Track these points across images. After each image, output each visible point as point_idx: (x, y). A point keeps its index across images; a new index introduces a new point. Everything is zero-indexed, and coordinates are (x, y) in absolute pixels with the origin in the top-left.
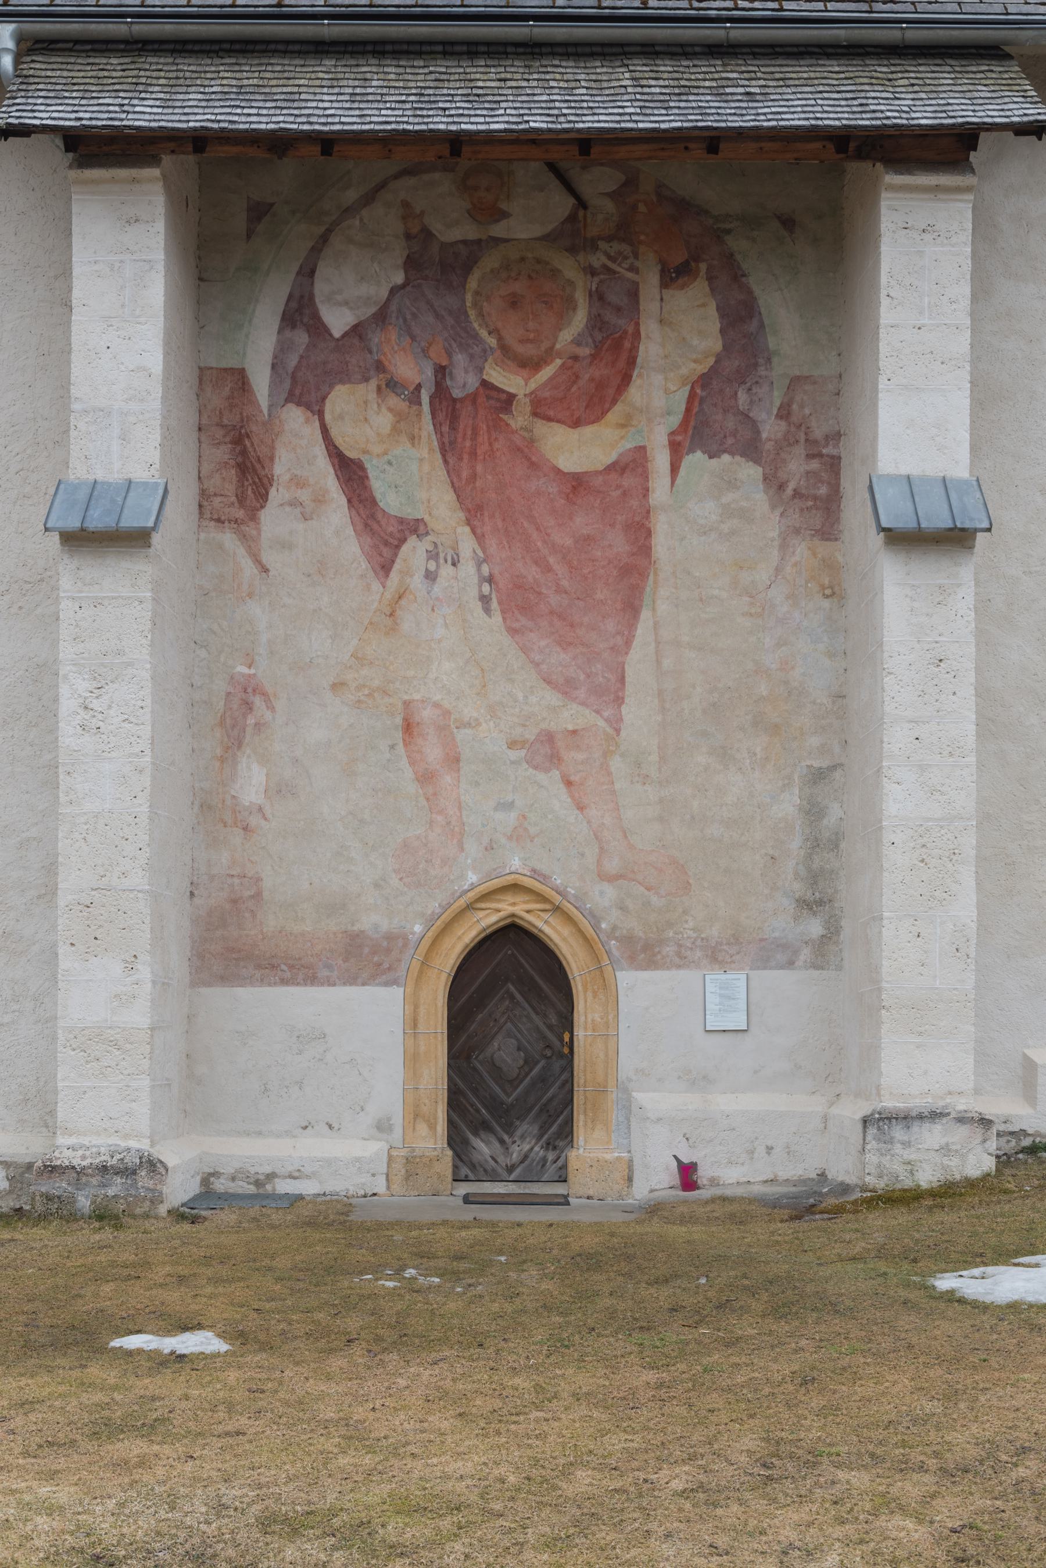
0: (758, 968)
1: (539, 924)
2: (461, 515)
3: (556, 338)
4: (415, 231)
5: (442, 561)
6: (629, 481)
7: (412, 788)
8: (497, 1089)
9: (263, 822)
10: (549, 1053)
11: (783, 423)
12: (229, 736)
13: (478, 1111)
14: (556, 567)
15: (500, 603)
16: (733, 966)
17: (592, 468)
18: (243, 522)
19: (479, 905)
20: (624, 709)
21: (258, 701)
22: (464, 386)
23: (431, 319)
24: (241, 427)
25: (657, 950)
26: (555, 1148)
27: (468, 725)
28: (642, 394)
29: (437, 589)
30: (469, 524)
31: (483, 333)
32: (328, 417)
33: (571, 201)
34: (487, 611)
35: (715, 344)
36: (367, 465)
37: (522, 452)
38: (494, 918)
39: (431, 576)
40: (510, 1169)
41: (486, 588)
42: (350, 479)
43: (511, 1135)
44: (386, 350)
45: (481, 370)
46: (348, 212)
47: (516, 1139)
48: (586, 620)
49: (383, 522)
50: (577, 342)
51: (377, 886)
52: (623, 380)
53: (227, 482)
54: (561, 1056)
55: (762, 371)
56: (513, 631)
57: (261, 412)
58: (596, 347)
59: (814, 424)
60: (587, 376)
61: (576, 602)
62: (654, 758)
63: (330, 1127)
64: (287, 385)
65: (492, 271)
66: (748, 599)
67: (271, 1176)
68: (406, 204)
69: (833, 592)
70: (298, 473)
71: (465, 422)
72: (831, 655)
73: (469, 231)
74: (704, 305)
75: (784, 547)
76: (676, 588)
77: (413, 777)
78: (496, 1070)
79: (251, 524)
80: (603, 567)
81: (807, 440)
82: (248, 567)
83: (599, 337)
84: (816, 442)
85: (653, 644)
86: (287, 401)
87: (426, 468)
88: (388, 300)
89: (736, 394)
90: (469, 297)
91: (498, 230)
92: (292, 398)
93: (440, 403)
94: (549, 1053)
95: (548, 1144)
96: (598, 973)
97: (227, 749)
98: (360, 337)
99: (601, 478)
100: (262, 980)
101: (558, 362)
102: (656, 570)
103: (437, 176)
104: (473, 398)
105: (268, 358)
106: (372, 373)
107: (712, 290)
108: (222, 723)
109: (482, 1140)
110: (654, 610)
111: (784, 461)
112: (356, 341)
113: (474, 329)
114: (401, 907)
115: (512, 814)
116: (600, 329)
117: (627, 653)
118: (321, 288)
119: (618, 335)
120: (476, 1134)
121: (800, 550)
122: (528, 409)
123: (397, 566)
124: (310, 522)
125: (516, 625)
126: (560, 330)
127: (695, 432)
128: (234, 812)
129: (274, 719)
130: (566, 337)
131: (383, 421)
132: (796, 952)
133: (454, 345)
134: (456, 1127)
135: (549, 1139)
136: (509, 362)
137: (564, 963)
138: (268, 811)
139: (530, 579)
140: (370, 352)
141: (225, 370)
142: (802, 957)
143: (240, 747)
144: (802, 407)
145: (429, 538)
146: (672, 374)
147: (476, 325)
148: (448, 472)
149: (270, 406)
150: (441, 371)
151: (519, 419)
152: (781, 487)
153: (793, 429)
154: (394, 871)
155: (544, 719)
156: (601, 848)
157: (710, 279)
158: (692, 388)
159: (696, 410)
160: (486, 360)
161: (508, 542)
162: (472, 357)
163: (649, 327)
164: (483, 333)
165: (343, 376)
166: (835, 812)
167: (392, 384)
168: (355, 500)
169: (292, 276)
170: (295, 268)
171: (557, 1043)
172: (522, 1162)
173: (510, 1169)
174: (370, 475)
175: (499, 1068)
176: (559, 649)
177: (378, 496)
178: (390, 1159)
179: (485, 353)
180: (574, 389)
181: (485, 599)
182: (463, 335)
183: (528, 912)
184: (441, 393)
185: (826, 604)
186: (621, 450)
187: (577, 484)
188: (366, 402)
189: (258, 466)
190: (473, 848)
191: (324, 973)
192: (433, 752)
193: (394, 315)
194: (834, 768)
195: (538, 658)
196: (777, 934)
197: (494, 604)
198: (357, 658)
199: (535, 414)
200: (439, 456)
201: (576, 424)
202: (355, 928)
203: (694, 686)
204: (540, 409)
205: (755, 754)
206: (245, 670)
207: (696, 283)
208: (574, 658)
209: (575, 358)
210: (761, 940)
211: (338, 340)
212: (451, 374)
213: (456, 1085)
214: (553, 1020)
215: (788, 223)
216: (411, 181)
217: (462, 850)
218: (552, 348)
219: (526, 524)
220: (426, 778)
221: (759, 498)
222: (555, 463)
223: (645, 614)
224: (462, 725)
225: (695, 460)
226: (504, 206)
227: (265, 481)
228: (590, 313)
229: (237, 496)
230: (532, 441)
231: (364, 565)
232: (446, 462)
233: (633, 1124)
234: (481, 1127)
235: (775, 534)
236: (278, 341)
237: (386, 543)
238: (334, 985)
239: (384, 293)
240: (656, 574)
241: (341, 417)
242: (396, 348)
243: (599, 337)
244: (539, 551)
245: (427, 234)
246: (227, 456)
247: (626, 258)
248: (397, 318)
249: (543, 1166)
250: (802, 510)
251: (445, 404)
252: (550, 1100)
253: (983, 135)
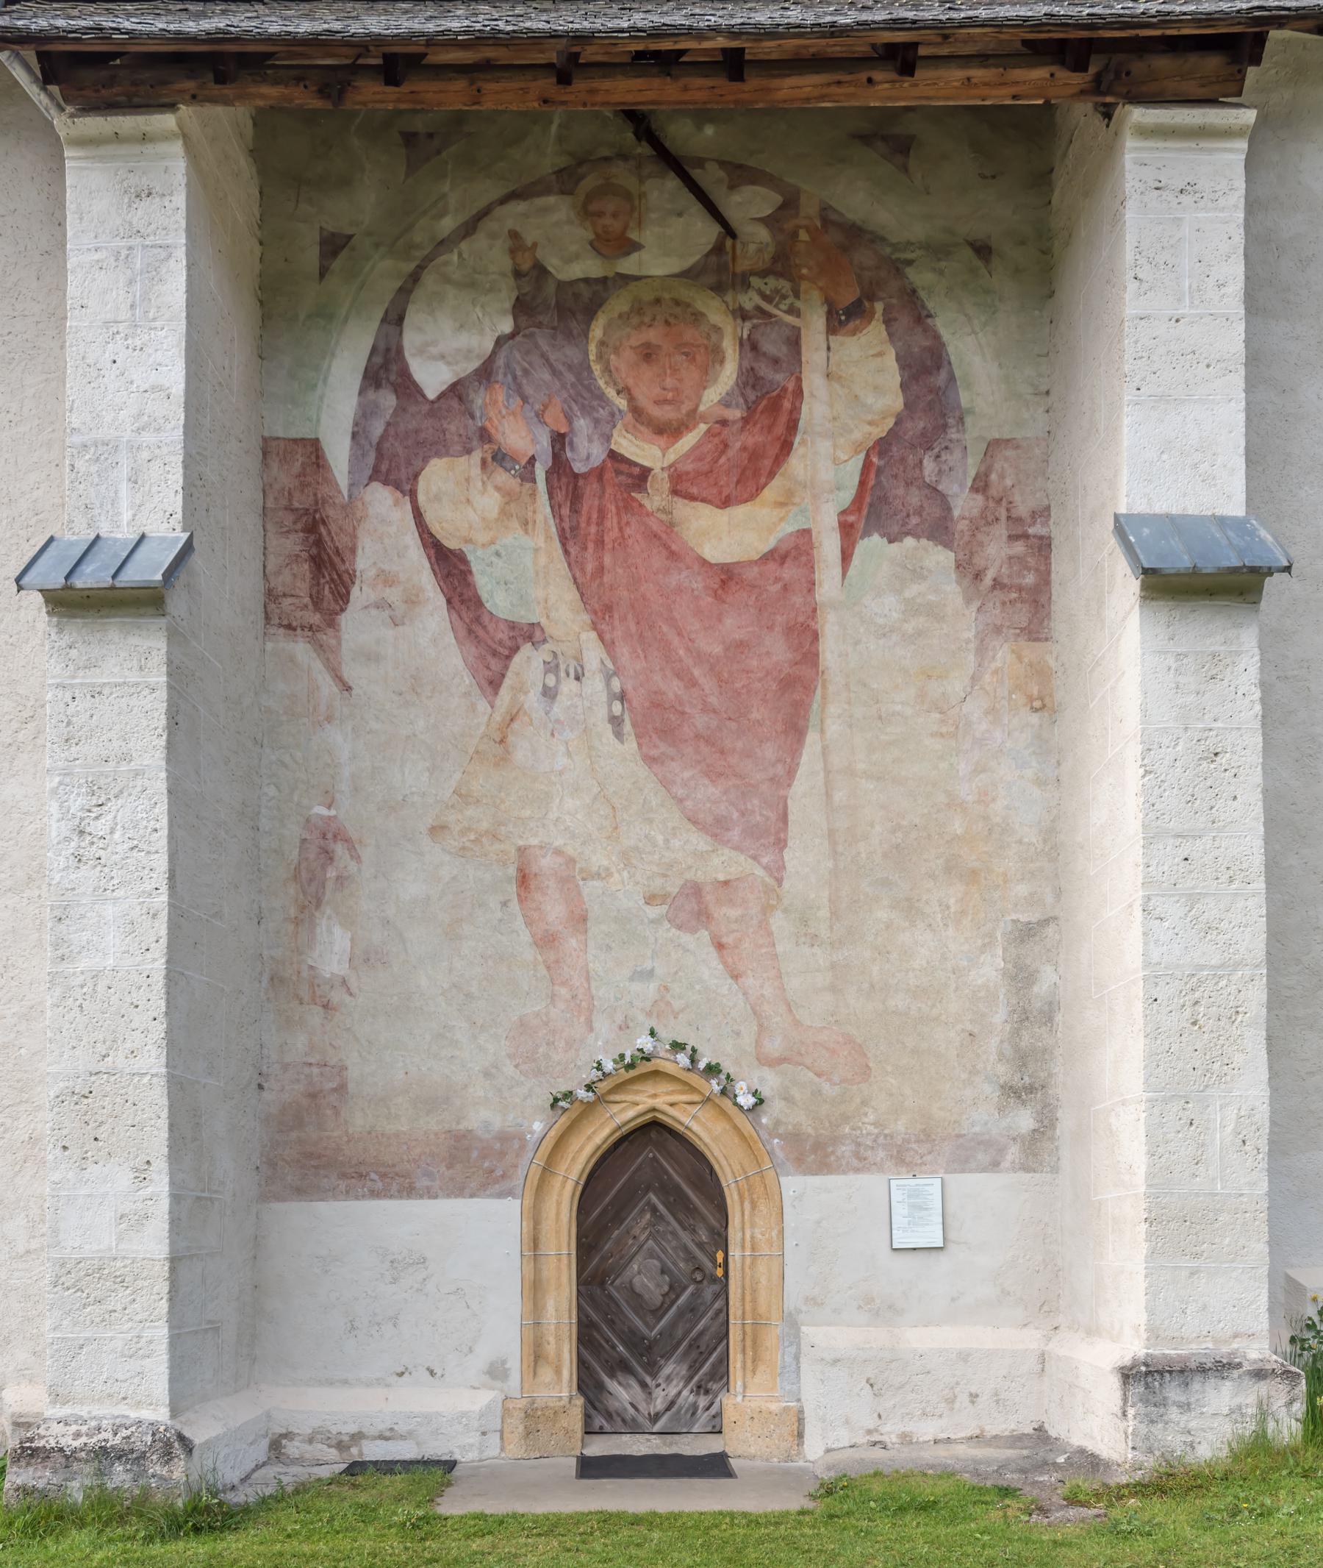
0: (955, 1171)
1: (686, 1120)
2: (586, 618)
3: (700, 398)
4: (525, 266)
5: (563, 674)
6: (789, 572)
7: (529, 954)
8: (638, 1323)
9: (348, 999)
10: (698, 1277)
11: (980, 498)
12: (304, 892)
13: (614, 1347)
14: (702, 681)
15: (634, 725)
16: (924, 1168)
17: (745, 558)
18: (319, 629)
19: (612, 1098)
20: (787, 854)
21: (339, 849)
22: (588, 458)
23: (546, 375)
24: (316, 511)
25: (830, 1149)
26: (707, 1392)
27: (597, 876)
28: (806, 466)
29: (557, 710)
30: (595, 629)
31: (611, 393)
32: (421, 498)
33: (714, 230)
34: (619, 735)
35: (894, 401)
36: (470, 557)
37: (660, 538)
38: (631, 1113)
39: (549, 694)
40: (655, 1418)
41: (617, 708)
42: (449, 575)
43: (654, 1376)
44: (492, 414)
45: (608, 438)
46: (443, 245)
47: (660, 1381)
48: (739, 744)
49: (491, 627)
50: (725, 403)
51: (487, 1074)
52: (782, 449)
53: (298, 579)
54: (714, 1280)
55: (953, 434)
56: (650, 760)
57: (340, 492)
58: (749, 408)
59: (1017, 498)
60: (738, 445)
61: (728, 723)
62: (824, 913)
63: (432, 1373)
64: (371, 458)
65: (620, 316)
66: (938, 716)
67: (357, 1437)
68: (514, 235)
69: (1043, 705)
70: (386, 567)
71: (589, 503)
72: (1040, 782)
73: (589, 267)
74: (880, 354)
75: (981, 650)
76: (849, 703)
77: (531, 940)
78: (635, 1297)
79: (330, 631)
80: (760, 680)
81: (1009, 518)
82: (327, 686)
83: (752, 396)
84: (1019, 520)
85: (822, 774)
86: (371, 479)
87: (543, 560)
88: (494, 353)
89: (921, 462)
90: (593, 349)
91: (628, 265)
92: (377, 475)
93: (559, 480)
94: (698, 1277)
95: (699, 1387)
96: (758, 1179)
97: (303, 908)
98: (460, 399)
99: (756, 569)
100: (347, 1192)
101: (703, 427)
102: (824, 682)
103: (551, 200)
104: (599, 473)
105: (347, 426)
106: (475, 443)
107: (890, 335)
108: (296, 877)
109: (620, 1384)
110: (822, 731)
111: (981, 544)
112: (455, 403)
113: (599, 388)
114: (517, 1100)
115: (652, 986)
116: (754, 387)
117: (789, 786)
118: (411, 339)
119: (775, 394)
120: (612, 1375)
121: (1003, 654)
122: (667, 486)
123: (507, 682)
124: (401, 628)
125: (654, 753)
126: (705, 388)
127: (871, 511)
128: (312, 985)
129: (359, 870)
130: (712, 396)
131: (490, 502)
132: (1002, 1151)
133: (575, 408)
134: (588, 1368)
135: (700, 1381)
136: (642, 428)
137: (716, 1167)
138: (353, 984)
139: (671, 696)
140: (473, 417)
141: (295, 441)
142: (1009, 1157)
143: (318, 905)
144: (1002, 476)
145: (547, 646)
146: (842, 440)
147: (601, 383)
148: (569, 565)
149: (352, 485)
150: (559, 440)
151: (655, 498)
152: (978, 576)
153: (991, 504)
154: (509, 1056)
155: (690, 867)
156: (761, 1026)
157: (888, 322)
158: (868, 456)
159: (872, 482)
160: (614, 426)
161: (643, 651)
162: (597, 422)
163: (813, 381)
164: (611, 393)
165: (439, 447)
166: (1048, 977)
167: (499, 456)
168: (456, 600)
169: (375, 324)
170: (379, 314)
171: (709, 1265)
172: (668, 1409)
173: (655, 1418)
174: (474, 569)
175: (639, 1296)
176: (706, 782)
177: (484, 596)
178: (506, 1412)
179: (613, 417)
180: (723, 460)
181: (615, 721)
182: (586, 395)
183: (672, 1105)
184: (559, 466)
185: (1035, 719)
186: (780, 535)
187: (727, 578)
188: (468, 480)
189: (337, 560)
190: (604, 1027)
191: (423, 1183)
192: (554, 911)
193: (501, 371)
194: (1045, 922)
195: (681, 792)
196: (977, 1129)
197: (627, 727)
198: (460, 795)
199: (675, 492)
200: (557, 544)
201: (725, 503)
202: (461, 1127)
203: (872, 825)
204: (681, 486)
205: (948, 907)
206: (322, 811)
207: (870, 327)
208: (726, 792)
209: (724, 423)
210: (959, 1136)
211: (432, 402)
212: (571, 443)
213: (587, 1317)
214: (704, 1238)
215: (983, 250)
216: (520, 207)
217: (591, 1029)
218: (695, 410)
219: (665, 628)
220: (547, 941)
221: (951, 590)
222: (699, 552)
223: (812, 737)
224: (589, 876)
225: (871, 546)
226: (633, 235)
227: (346, 577)
228: (740, 366)
229: (311, 596)
230: (671, 526)
231: (468, 680)
232: (566, 552)
233: (804, 1366)
234: (620, 1367)
235: (970, 634)
236: (360, 404)
237: (495, 654)
238: (436, 1197)
239: (489, 345)
240: (824, 687)
241: (437, 498)
242: (504, 412)
243: (752, 396)
244: (681, 661)
245: (541, 271)
246: (298, 548)
247: (784, 297)
248: (505, 375)
249: (693, 1414)
250: (1004, 603)
251: (564, 480)
252: (701, 1333)
253: (1276, 35)
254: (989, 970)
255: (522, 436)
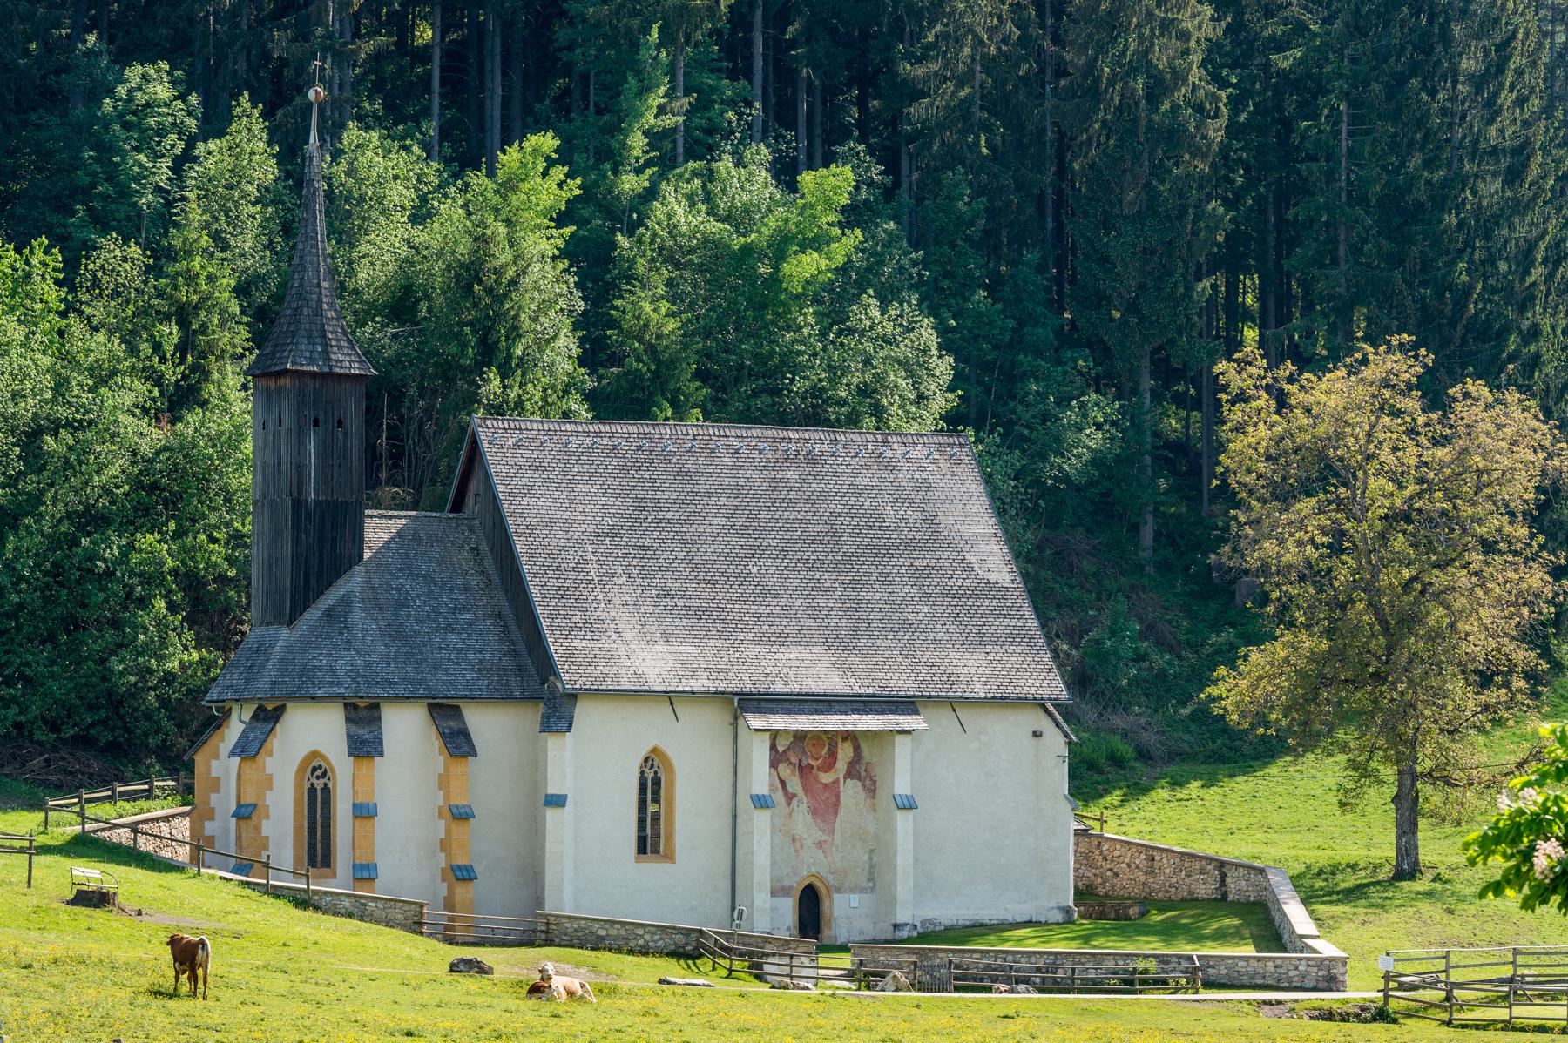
254: (866, 857)
255: (794, 760)
